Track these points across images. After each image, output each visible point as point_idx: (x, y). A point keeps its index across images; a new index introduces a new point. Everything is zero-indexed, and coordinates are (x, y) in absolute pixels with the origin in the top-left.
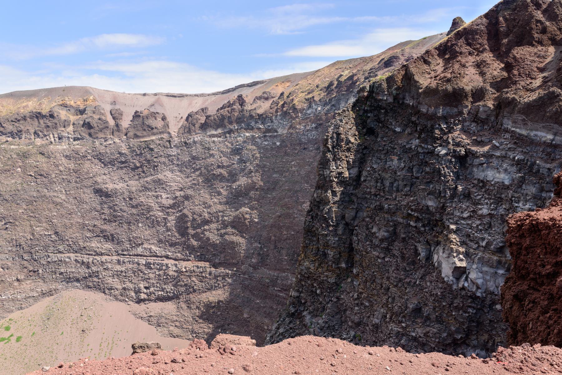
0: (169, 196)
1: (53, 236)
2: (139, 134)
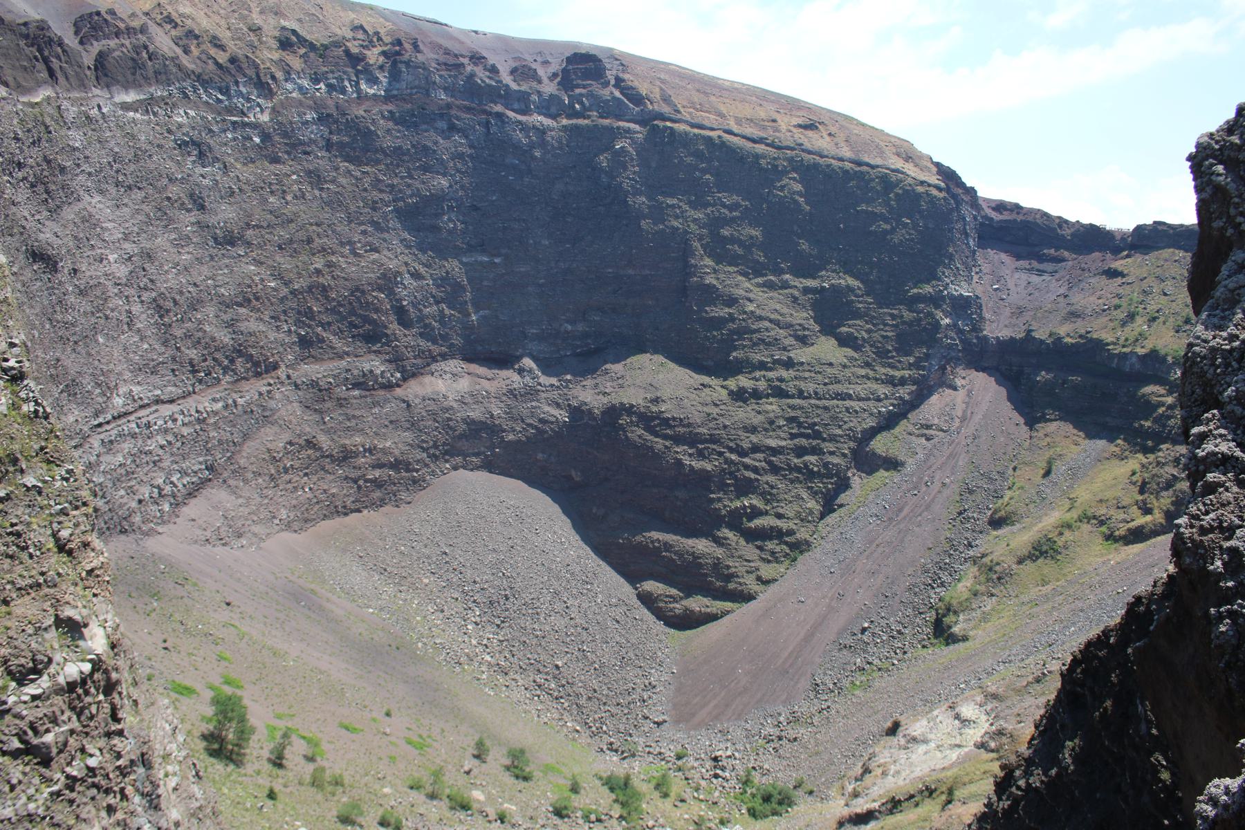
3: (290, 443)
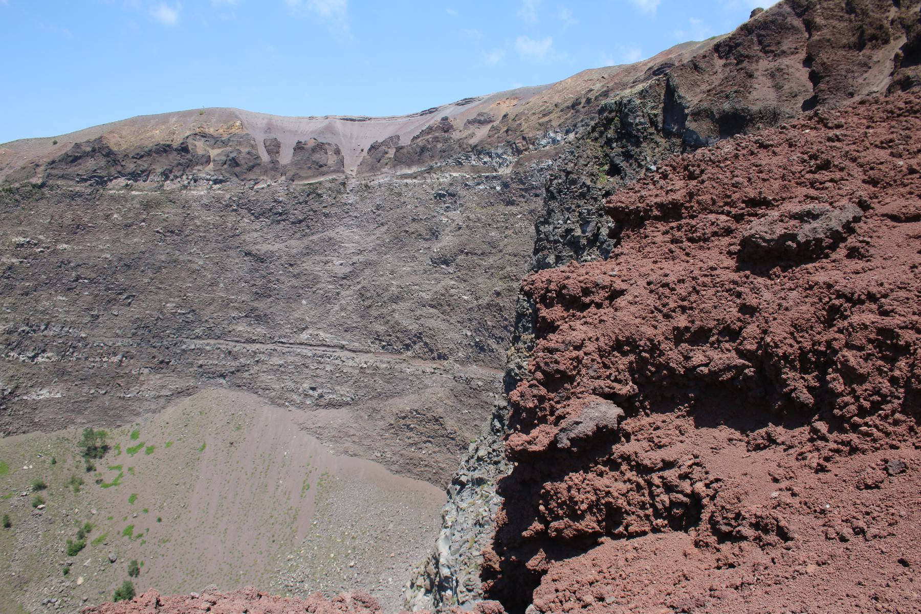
0: (344, 261)
1: (188, 316)
2: (302, 174)
3: (416, 411)
